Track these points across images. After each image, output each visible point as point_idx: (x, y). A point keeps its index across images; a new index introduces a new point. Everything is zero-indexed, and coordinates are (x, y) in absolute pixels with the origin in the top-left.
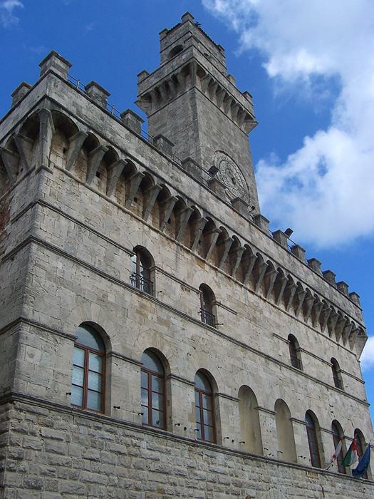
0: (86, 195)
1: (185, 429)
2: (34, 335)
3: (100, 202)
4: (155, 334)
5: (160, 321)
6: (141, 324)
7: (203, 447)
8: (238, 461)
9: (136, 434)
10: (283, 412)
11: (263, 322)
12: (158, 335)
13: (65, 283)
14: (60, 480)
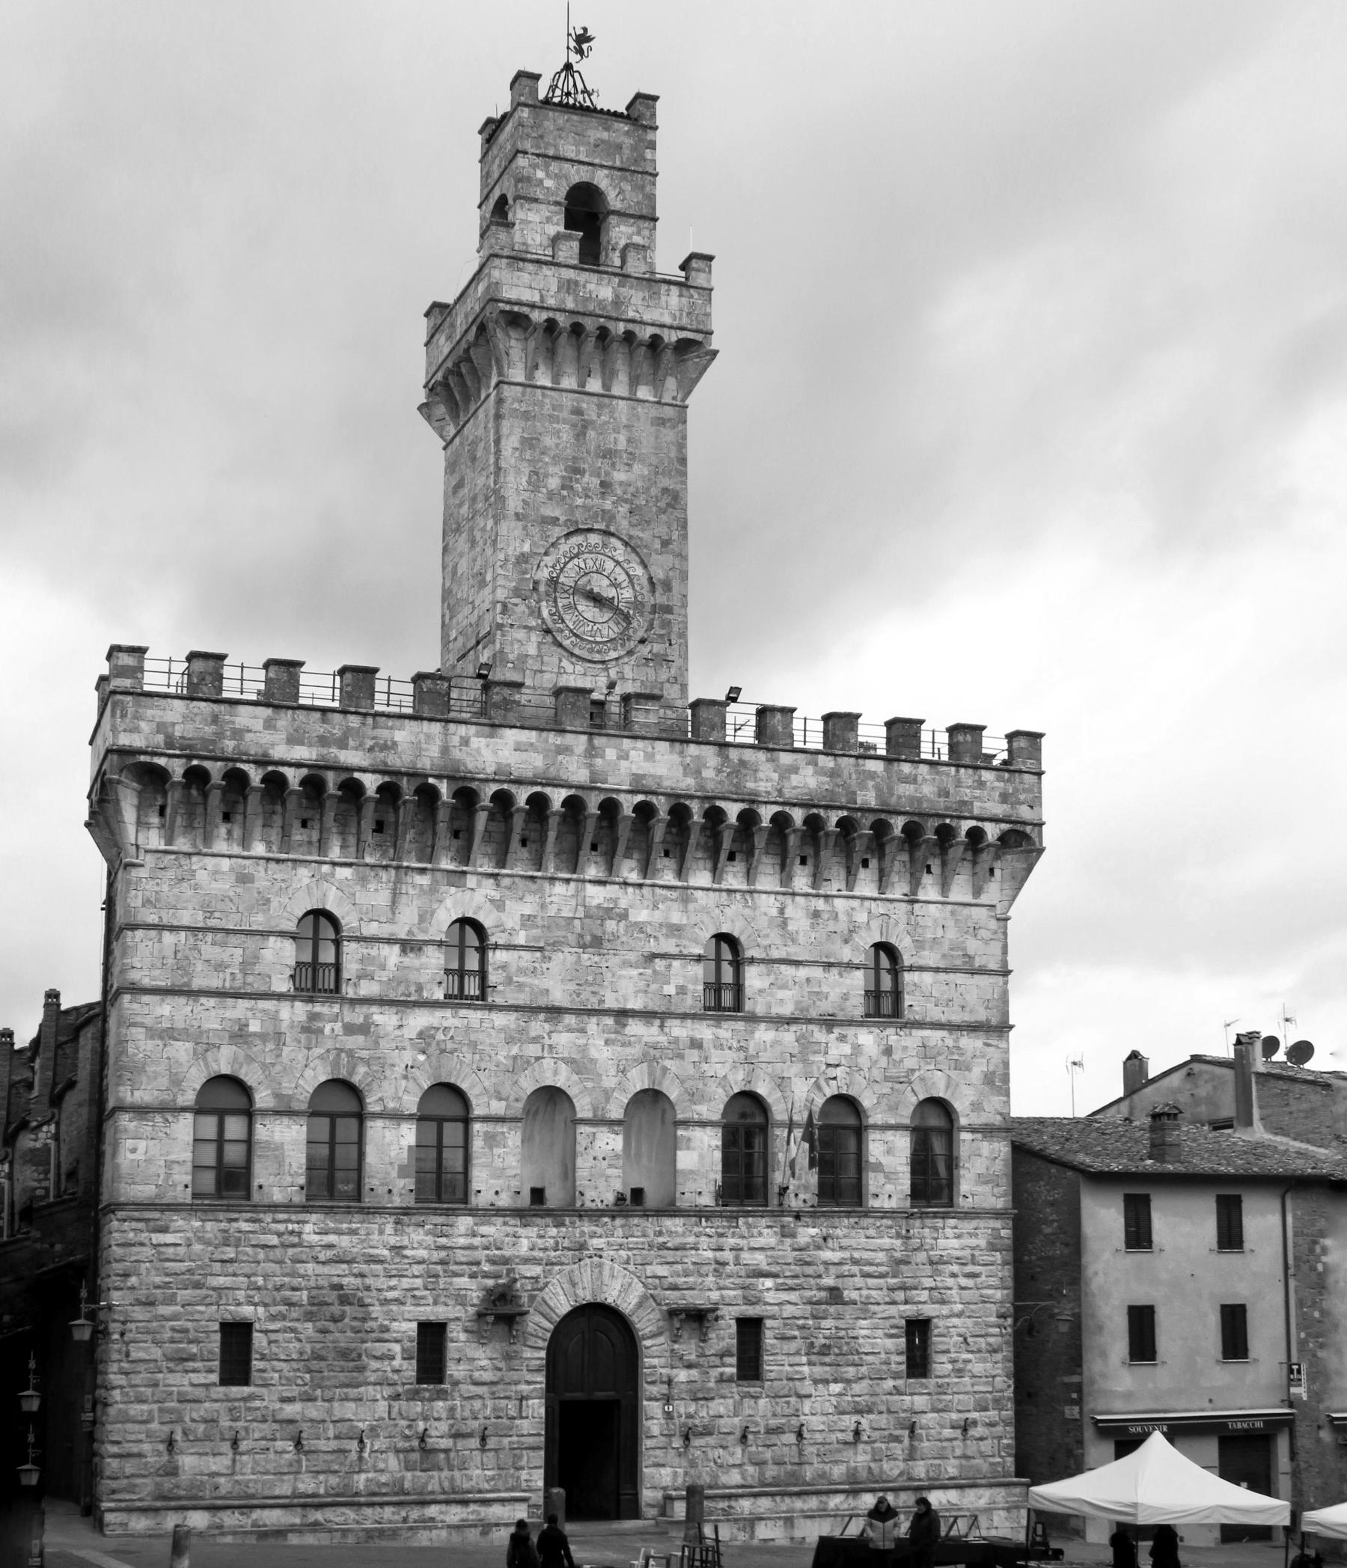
0: (203, 869)
1: (390, 1191)
3: (232, 869)
4: (338, 1055)
5: (350, 1029)
6: (309, 1049)
7: (422, 1214)
8: (505, 1224)
9: (293, 1217)
10: (664, 1111)
11: (624, 939)
12: (343, 1055)
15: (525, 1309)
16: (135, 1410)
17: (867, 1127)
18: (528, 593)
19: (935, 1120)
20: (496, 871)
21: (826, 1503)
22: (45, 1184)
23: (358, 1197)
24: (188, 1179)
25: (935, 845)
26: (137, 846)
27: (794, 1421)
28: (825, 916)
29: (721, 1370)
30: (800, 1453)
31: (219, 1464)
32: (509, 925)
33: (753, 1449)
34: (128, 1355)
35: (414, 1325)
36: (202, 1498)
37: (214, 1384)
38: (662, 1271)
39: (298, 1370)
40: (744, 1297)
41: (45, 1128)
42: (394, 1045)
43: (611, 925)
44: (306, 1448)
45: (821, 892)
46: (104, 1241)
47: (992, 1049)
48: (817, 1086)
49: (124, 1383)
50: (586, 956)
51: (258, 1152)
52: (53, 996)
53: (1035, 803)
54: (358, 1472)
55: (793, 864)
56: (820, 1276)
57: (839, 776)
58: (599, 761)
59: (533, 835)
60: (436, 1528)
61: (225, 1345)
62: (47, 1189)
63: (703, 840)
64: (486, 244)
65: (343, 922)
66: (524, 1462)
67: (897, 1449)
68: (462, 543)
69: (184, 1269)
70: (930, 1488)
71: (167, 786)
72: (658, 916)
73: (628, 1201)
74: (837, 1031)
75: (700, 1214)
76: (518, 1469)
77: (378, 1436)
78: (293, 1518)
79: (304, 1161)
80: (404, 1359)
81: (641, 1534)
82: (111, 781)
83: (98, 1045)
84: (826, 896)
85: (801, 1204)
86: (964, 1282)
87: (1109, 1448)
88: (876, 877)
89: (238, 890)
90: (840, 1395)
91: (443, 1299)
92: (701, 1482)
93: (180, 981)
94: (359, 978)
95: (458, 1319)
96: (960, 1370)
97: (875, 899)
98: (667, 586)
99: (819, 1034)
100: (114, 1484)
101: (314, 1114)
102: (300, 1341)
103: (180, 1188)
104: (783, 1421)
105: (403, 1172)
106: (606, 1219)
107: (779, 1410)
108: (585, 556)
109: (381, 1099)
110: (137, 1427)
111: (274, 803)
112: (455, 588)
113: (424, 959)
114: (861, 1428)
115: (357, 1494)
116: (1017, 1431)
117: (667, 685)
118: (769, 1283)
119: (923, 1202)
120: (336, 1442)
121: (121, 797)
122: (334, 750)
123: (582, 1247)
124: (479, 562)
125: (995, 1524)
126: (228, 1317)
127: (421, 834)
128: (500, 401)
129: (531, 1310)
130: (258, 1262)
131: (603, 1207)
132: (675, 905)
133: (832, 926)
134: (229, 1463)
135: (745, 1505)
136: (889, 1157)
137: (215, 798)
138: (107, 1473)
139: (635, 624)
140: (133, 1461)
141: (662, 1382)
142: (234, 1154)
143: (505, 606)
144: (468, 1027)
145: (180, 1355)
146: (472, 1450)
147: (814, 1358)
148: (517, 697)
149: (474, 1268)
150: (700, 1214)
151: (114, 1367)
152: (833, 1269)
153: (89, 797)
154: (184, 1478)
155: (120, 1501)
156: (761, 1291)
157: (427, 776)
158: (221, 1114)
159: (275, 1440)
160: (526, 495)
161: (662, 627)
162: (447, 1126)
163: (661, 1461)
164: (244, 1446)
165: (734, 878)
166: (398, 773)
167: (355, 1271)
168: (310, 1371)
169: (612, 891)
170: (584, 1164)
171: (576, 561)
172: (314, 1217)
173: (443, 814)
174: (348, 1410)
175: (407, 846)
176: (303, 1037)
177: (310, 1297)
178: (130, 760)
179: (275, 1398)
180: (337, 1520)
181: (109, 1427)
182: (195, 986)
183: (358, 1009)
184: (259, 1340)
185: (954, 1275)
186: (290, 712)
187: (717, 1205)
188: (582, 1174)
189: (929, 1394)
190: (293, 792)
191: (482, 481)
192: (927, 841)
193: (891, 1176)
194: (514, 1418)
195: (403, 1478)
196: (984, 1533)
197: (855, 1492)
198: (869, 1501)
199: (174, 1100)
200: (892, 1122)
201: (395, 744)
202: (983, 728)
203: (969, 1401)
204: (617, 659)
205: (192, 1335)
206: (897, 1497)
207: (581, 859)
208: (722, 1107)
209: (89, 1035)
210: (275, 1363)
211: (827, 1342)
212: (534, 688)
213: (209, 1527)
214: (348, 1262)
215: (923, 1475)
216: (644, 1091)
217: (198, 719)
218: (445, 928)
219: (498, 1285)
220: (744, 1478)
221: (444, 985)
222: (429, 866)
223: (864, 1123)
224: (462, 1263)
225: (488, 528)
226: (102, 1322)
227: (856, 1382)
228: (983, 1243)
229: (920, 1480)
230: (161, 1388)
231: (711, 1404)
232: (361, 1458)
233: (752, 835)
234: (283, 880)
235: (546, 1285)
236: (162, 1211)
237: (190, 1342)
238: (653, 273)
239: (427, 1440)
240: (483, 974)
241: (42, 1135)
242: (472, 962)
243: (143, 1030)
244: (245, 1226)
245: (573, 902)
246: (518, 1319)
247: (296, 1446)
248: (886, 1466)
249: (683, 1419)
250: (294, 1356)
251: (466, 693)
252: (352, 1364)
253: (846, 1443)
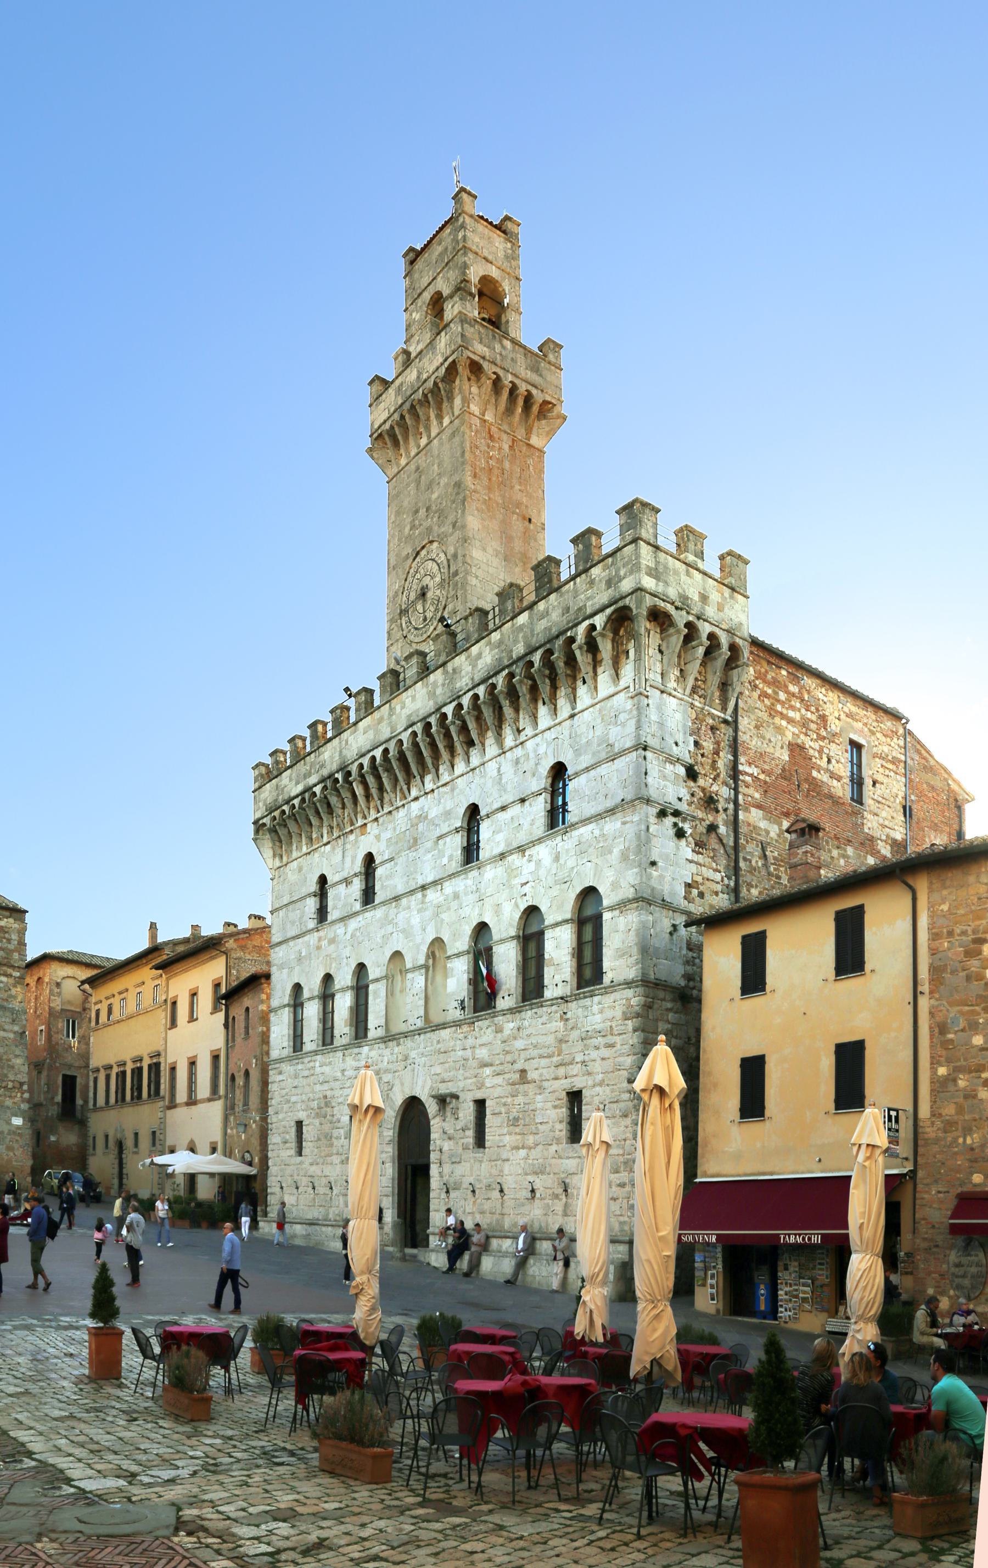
38: (438, 1069)
43: (421, 827)
72: (441, 809)
75: (457, 1024)
86: (605, 1052)
99: (514, 859)
118: (488, 1071)
150: (457, 1024)
152: (524, 1055)
200: (560, 919)
228: (618, 1013)
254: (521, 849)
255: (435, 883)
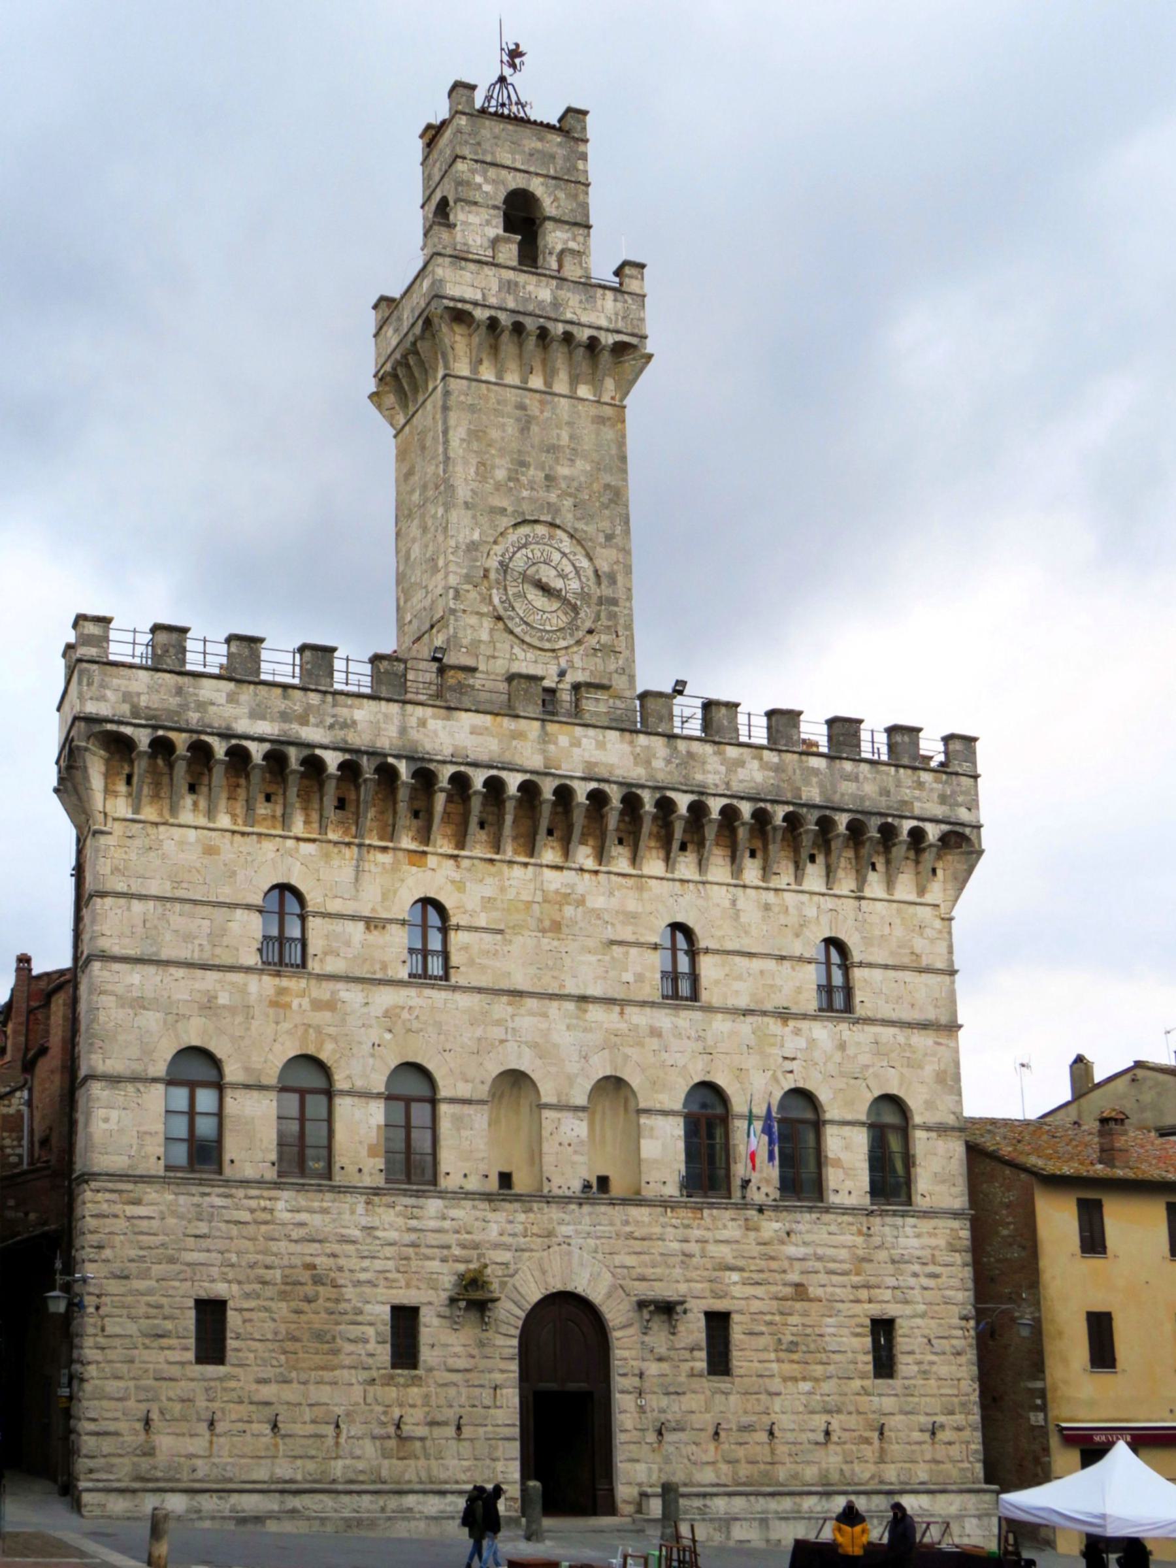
1: (360, 1170)
2: (106, 1093)
3: (198, 841)
4: (306, 1031)
5: (317, 1005)
6: (277, 1023)
8: (474, 1207)
9: (266, 1193)
11: (582, 924)
12: (311, 1031)
13: (146, 1004)
14: (155, 1267)
15: (496, 1295)
16: (113, 1386)
17: (825, 1122)
18: (479, 580)
19: (890, 1117)
20: (456, 852)
21: (800, 1505)
22: (18, 1151)
23: (328, 1174)
24: (160, 1151)
25: (879, 843)
26: (105, 814)
27: (767, 1420)
28: (776, 909)
29: (691, 1364)
30: (773, 1452)
31: (198, 1445)
32: (469, 907)
33: (726, 1446)
34: (103, 1330)
35: (388, 1308)
36: (178, 1480)
37: (190, 1363)
38: (630, 1261)
39: (273, 1350)
40: (712, 1291)
41: (18, 1094)
42: (360, 1023)
43: (569, 911)
44: (283, 1432)
45: (771, 885)
46: (79, 1212)
47: (942, 1048)
48: (775, 1079)
49: (99, 1358)
50: (546, 941)
51: (228, 1125)
52: (24, 961)
53: (973, 805)
54: (336, 1458)
55: (742, 857)
56: (784, 1272)
57: (783, 771)
58: (552, 747)
59: (490, 818)
60: (415, 1519)
61: (199, 1322)
62: (20, 1156)
63: (655, 830)
64: (430, 242)
65: (308, 897)
66: (499, 1453)
67: (869, 1452)
68: (414, 530)
69: (158, 1243)
70: (902, 1492)
71: (134, 755)
72: (614, 903)
73: (595, 1189)
74: (791, 1023)
75: (665, 1204)
76: (494, 1460)
77: (353, 1421)
78: (271, 1504)
79: (275, 1136)
80: (379, 1343)
81: (619, 1531)
82: (78, 747)
83: (69, 1011)
84: (776, 890)
85: (763, 1197)
86: (925, 1282)
87: (1075, 1456)
88: (823, 873)
89: (205, 861)
90: (810, 1393)
91: (414, 1283)
92: (675, 1479)
93: (147, 950)
94: (325, 954)
95: (430, 1303)
96: (925, 1372)
97: (823, 895)
98: (613, 580)
100: (90, 1463)
101: (283, 1089)
102: (274, 1320)
103: (153, 1159)
104: (754, 1418)
105: (372, 1152)
106: (573, 1207)
107: (749, 1406)
108: (532, 547)
109: (349, 1077)
110: (113, 1404)
111: (238, 776)
112: (409, 572)
113: (387, 937)
114: (831, 1428)
115: (334, 1481)
116: (984, 1436)
117: (615, 676)
118: (735, 1277)
119: (882, 1200)
120: (313, 1426)
121: (89, 764)
122: (295, 727)
123: (550, 1234)
124: (431, 548)
125: (967, 1531)
126: (203, 1295)
127: (382, 813)
128: (447, 393)
129: (503, 1296)
130: (231, 1239)
131: (569, 1193)
132: (631, 893)
133: (783, 920)
134: (207, 1445)
135: (720, 1505)
136: (847, 1154)
137: (181, 768)
138: (84, 1451)
139: (582, 614)
140: (109, 1439)
141: (634, 1375)
142: (206, 1127)
143: (457, 591)
144: (433, 1008)
145: (155, 1332)
146: (447, 1439)
147: (782, 1355)
148: (471, 681)
149: (445, 1252)
150: (665, 1204)
151: (88, 1342)
152: (798, 1265)
153: (57, 762)
154: (161, 1458)
155: (98, 1480)
156: (728, 1285)
157: (385, 755)
158: (193, 1086)
159: (251, 1422)
160: (474, 485)
161: (609, 619)
162: (415, 1106)
163: (636, 1457)
164: (220, 1427)
165: (686, 866)
166: (357, 752)
167: (328, 1251)
168: (285, 1352)
169: (569, 876)
170: (549, 1147)
171: (524, 551)
172: (286, 1194)
173: (403, 794)
174: (323, 1394)
175: (368, 823)
176: (271, 1011)
177: (285, 1276)
178: (97, 728)
179: (251, 1378)
180: (315, 1507)
181: (85, 1403)
182: (164, 957)
183: (324, 984)
184: (233, 1319)
185: (915, 1275)
186: (252, 687)
187: (682, 1195)
188: (548, 1160)
189: (896, 1395)
190: (257, 765)
191: (431, 470)
192: (870, 838)
193: (848, 1172)
194: (489, 1407)
195: (380, 1466)
196: (957, 1541)
197: (828, 1494)
198: (839, 1503)
199: (145, 1070)
200: (849, 1117)
201: (354, 723)
202: (919, 730)
203: (934, 1404)
204: (566, 648)
205: (167, 1311)
206: (869, 1501)
207: (539, 844)
208: (683, 1096)
209: (61, 1001)
210: (250, 1342)
211: (795, 1339)
212: (487, 673)
213: (188, 1511)
214: (320, 1241)
215: (894, 1479)
216: (607, 1078)
217: (163, 690)
218: (407, 907)
219: (469, 1270)
220: (718, 1477)
221: (408, 964)
222: (390, 845)
223: (822, 1118)
224: (433, 1247)
225: (439, 515)
226: (78, 1295)
227: (824, 1380)
228: (941, 1242)
229: (891, 1484)
230: (137, 1365)
231: (682, 1398)
232: (337, 1444)
233: (702, 826)
234: (249, 854)
235: (516, 1271)
236: (135, 1183)
237: (165, 1318)
238: (589, 278)
239: (402, 1426)
240: (445, 954)
241: (15, 1101)
242: (435, 943)
243: (114, 998)
244: (219, 1201)
245: (532, 886)
246: (490, 1305)
247: (273, 1429)
248: (857, 1468)
249: (655, 1414)
250: (270, 1336)
251: (423, 675)
252: (326, 1346)
253: (817, 1443)
254: (784, 1015)
255: (609, 1001)
